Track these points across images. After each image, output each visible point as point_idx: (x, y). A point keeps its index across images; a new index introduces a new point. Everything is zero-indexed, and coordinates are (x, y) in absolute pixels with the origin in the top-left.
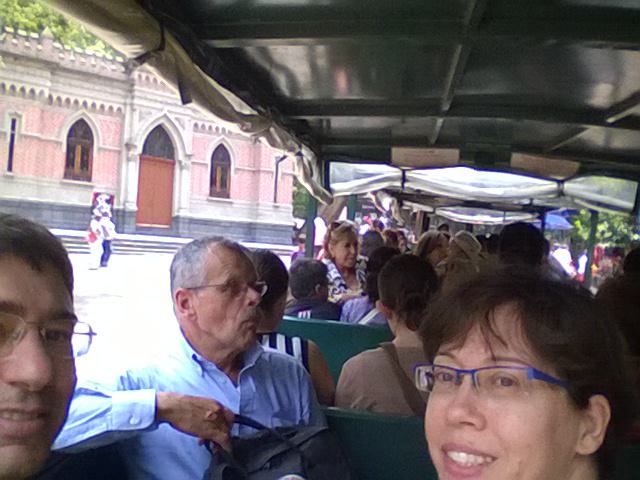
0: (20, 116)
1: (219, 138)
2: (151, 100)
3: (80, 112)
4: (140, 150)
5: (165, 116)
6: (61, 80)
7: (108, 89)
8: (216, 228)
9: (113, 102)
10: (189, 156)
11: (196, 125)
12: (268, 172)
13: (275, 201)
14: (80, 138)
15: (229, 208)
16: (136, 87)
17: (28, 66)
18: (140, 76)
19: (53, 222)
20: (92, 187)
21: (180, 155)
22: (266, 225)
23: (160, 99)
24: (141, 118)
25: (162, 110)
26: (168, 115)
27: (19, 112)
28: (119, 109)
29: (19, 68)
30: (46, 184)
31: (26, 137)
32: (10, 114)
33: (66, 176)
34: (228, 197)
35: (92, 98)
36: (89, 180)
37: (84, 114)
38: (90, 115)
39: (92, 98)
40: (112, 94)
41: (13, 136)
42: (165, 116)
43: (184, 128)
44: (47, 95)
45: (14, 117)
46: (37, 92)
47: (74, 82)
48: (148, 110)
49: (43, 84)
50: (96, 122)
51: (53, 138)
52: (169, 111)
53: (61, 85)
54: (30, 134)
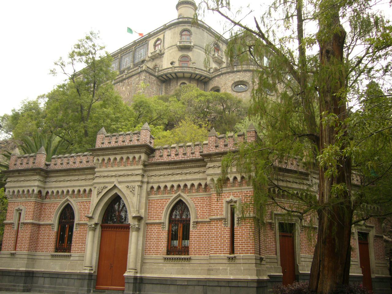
0: (21, 210)
1: (175, 196)
2: (107, 176)
3: (65, 199)
4: (96, 219)
5: (115, 187)
6: (55, 179)
7: (83, 177)
8: (172, 288)
9: (86, 186)
10: (139, 219)
11: (152, 188)
12: (220, 220)
13: (232, 251)
14: (67, 215)
15: (187, 267)
16: (96, 170)
17: (27, 176)
18: (98, 160)
19: (44, 287)
20: (70, 256)
21: (130, 221)
22: (218, 281)
23: (113, 174)
24: (99, 193)
25: (113, 182)
26: (117, 185)
27: (22, 207)
28: (90, 190)
29: (23, 178)
30: (43, 258)
31: (24, 224)
32: (17, 210)
33: (57, 249)
34: (188, 255)
35: (71, 187)
36: (69, 249)
37: (67, 200)
38: (70, 199)
39: (71, 187)
40: (85, 180)
41: (19, 223)
42: (115, 187)
43: (132, 192)
44: (36, 192)
45: (20, 212)
46: (31, 192)
47: (62, 178)
48: (102, 185)
49: (33, 184)
50: (75, 204)
51: (50, 222)
52: (120, 182)
53: (54, 183)
54: (26, 221)
